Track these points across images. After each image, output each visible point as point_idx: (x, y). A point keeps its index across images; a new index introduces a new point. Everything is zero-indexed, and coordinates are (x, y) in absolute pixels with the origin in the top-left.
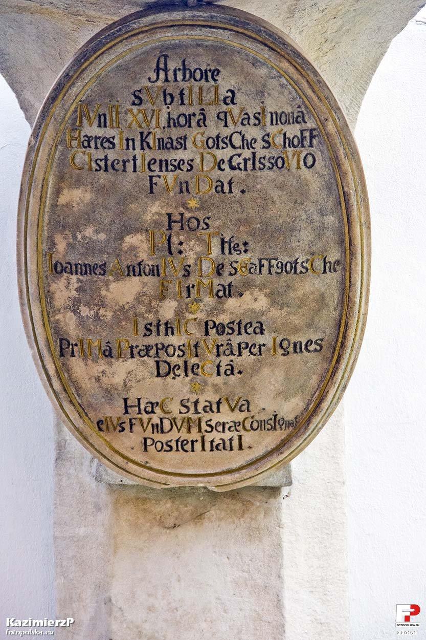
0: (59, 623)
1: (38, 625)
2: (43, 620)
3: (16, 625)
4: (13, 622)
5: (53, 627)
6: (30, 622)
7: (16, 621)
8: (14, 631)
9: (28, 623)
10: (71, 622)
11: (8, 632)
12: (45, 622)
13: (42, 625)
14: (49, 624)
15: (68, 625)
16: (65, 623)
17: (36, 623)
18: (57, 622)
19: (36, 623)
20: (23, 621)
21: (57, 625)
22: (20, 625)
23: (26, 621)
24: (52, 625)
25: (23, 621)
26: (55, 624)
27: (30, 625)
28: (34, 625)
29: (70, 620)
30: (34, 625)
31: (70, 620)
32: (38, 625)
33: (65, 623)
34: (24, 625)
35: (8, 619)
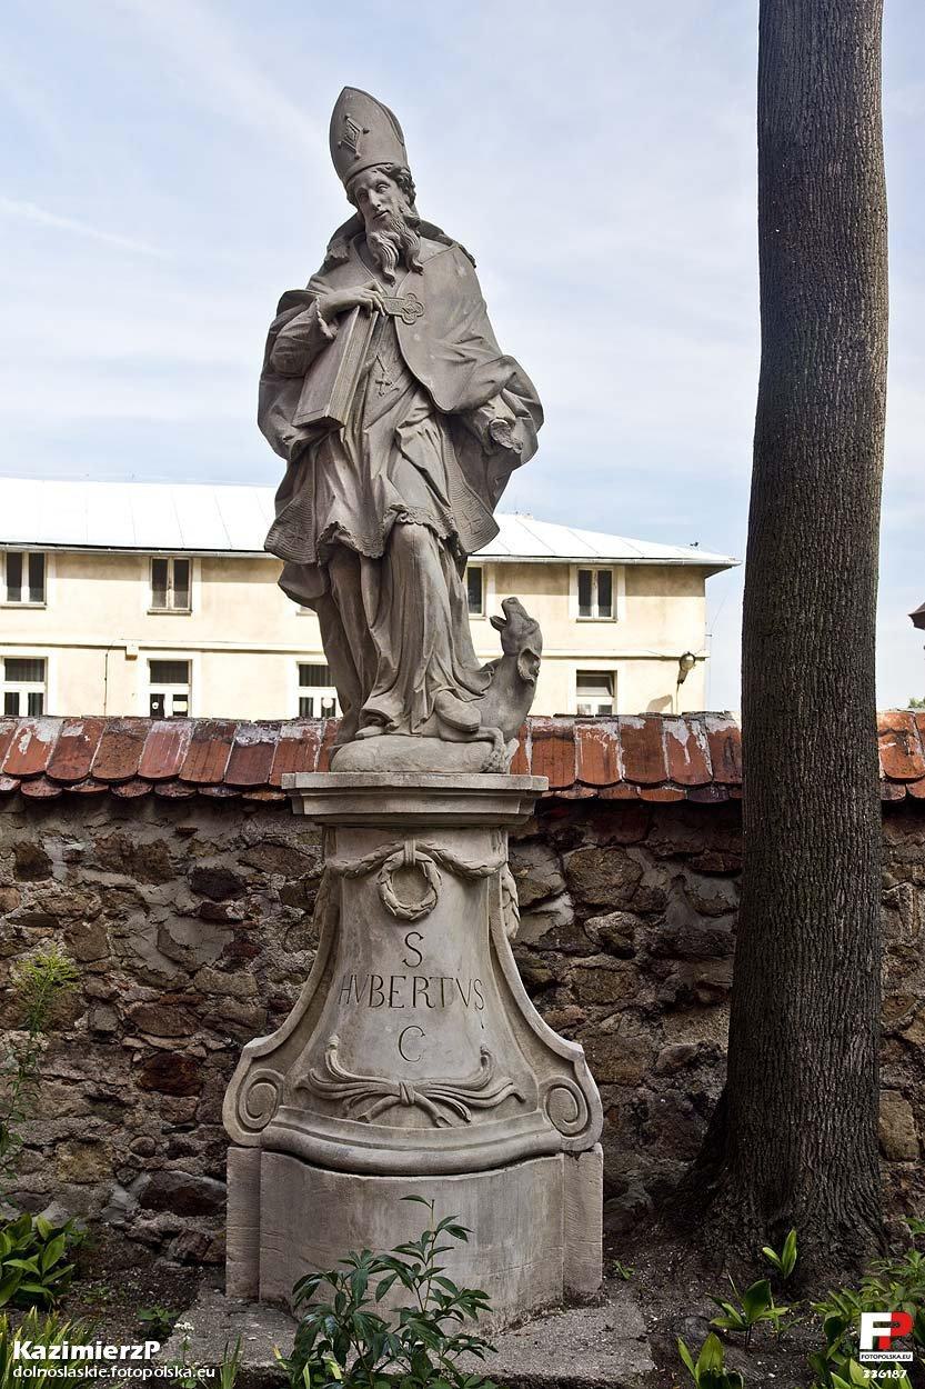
0: (128, 1353)
1: (82, 1357)
2: (94, 1345)
3: (35, 1356)
4: (28, 1350)
5: (117, 1360)
6: (66, 1349)
7: (36, 1348)
8: (130, 1369)
10: (153, 1351)
11: (116, 1373)
12: (99, 1348)
14: (107, 1356)
15: (147, 1357)
16: (142, 1353)
17: (78, 1352)
18: (124, 1349)
19: (78, 1352)
21: (123, 1356)
22: (43, 1357)
23: (57, 1349)
24: (114, 1357)
26: (119, 1351)
27: (65, 1357)
28: (74, 1356)
29: (152, 1347)
30: (74, 1356)
31: (152, 1347)
32: (82, 1357)
33: (142, 1353)
34: (52, 1356)
35: (17, 1344)
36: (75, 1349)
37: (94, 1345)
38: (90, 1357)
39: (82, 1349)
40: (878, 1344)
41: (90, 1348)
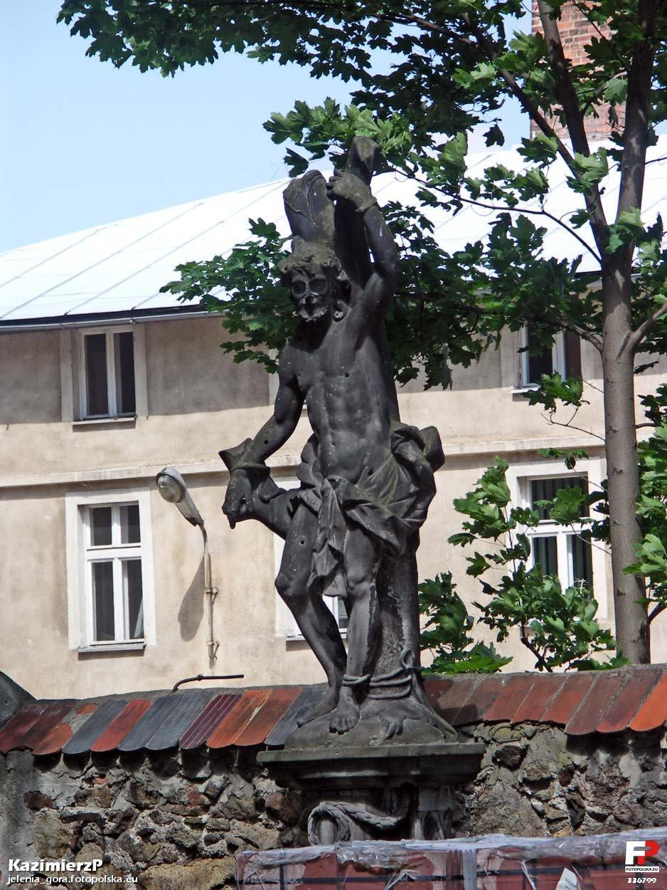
1: (53, 869)
6: (42, 864)
9: (38, 867)
12: (63, 864)
13: (58, 869)
17: (50, 867)
19: (50, 867)
20: (33, 863)
22: (28, 870)
23: (37, 864)
25: (33, 863)
27: (42, 869)
28: (47, 869)
30: (47, 869)
32: (53, 869)
34: (33, 869)
36: (48, 865)
37: (60, 862)
38: (58, 869)
39: (52, 864)
40: (636, 859)
41: (57, 864)
